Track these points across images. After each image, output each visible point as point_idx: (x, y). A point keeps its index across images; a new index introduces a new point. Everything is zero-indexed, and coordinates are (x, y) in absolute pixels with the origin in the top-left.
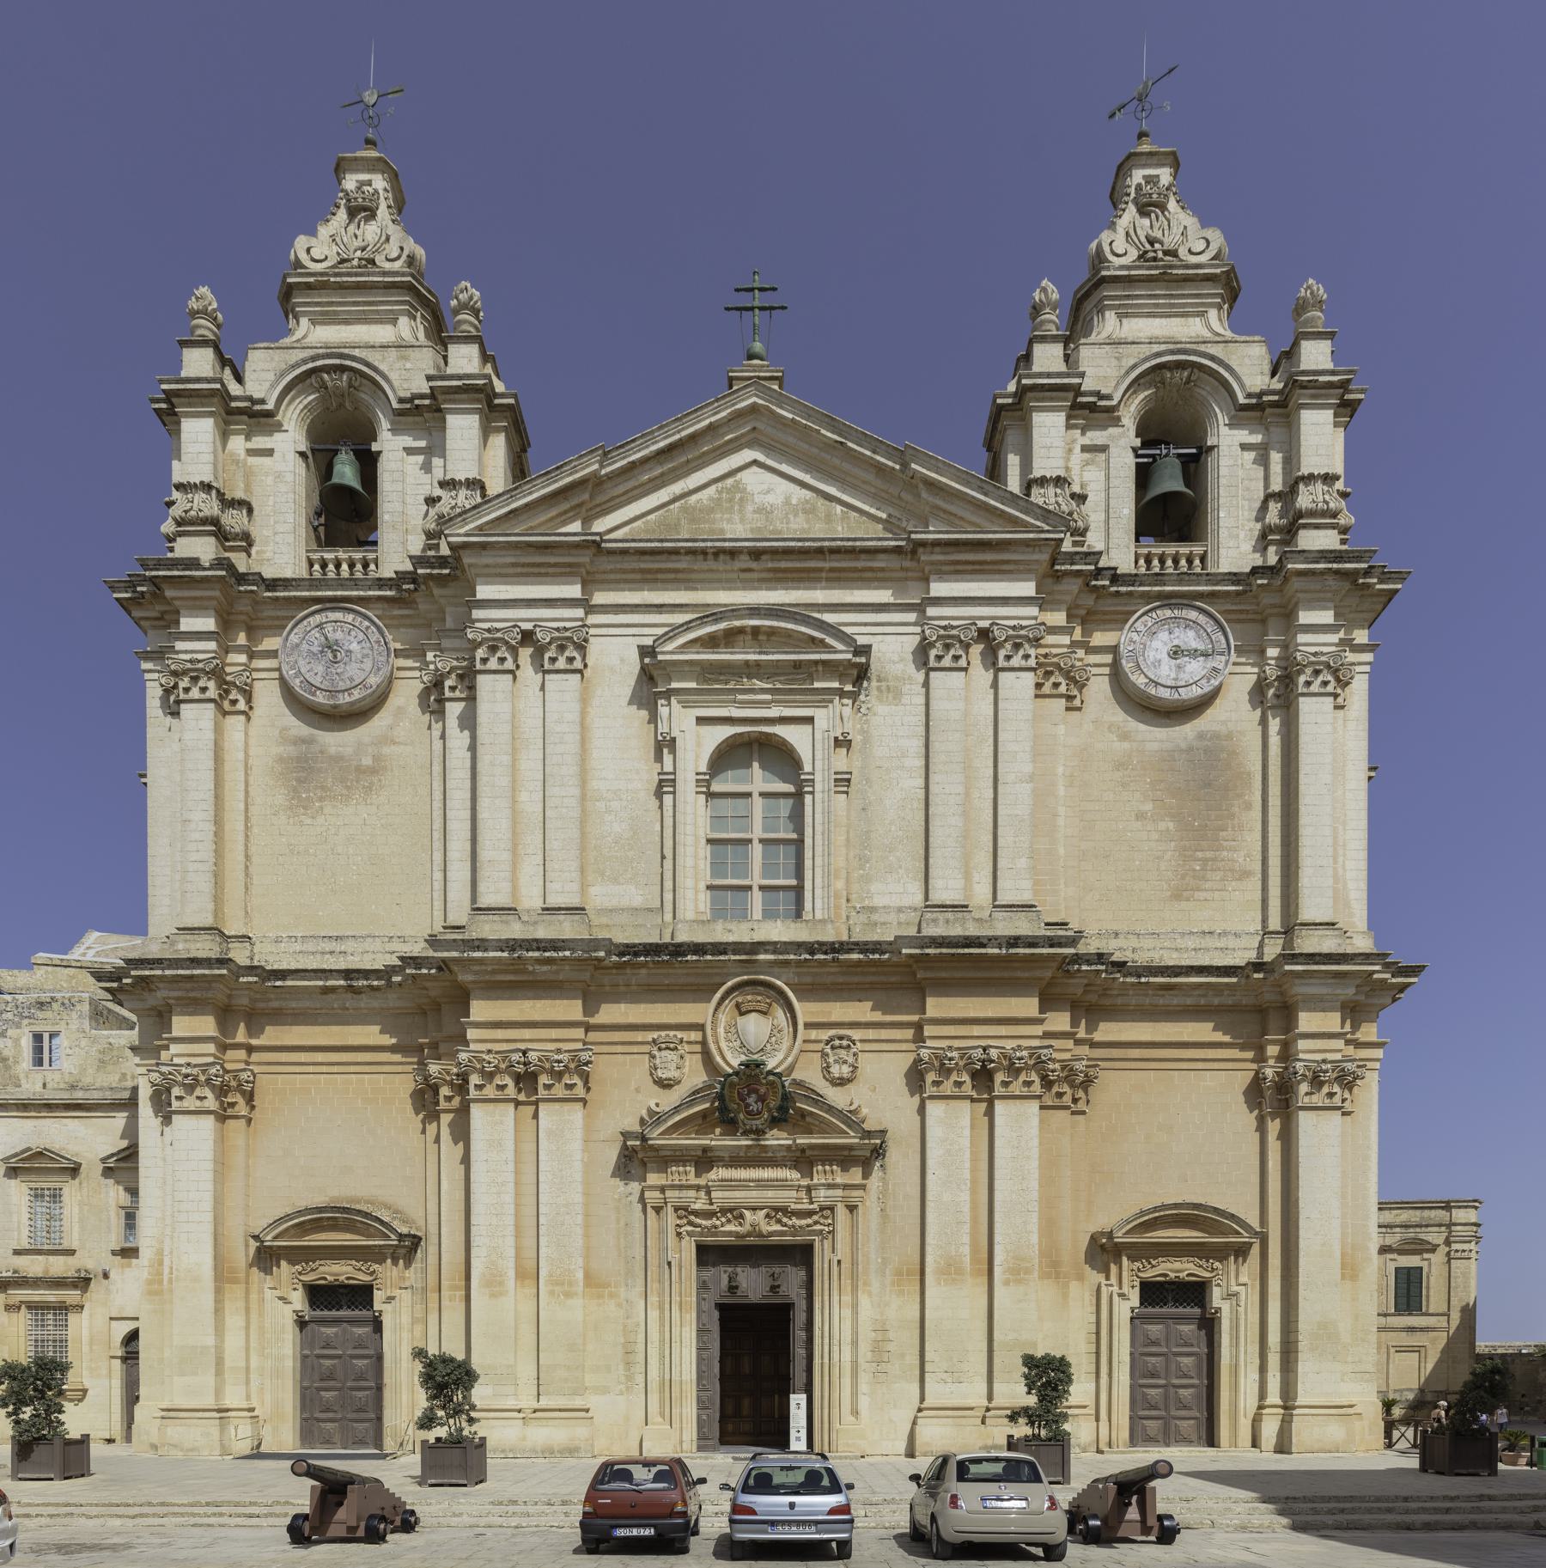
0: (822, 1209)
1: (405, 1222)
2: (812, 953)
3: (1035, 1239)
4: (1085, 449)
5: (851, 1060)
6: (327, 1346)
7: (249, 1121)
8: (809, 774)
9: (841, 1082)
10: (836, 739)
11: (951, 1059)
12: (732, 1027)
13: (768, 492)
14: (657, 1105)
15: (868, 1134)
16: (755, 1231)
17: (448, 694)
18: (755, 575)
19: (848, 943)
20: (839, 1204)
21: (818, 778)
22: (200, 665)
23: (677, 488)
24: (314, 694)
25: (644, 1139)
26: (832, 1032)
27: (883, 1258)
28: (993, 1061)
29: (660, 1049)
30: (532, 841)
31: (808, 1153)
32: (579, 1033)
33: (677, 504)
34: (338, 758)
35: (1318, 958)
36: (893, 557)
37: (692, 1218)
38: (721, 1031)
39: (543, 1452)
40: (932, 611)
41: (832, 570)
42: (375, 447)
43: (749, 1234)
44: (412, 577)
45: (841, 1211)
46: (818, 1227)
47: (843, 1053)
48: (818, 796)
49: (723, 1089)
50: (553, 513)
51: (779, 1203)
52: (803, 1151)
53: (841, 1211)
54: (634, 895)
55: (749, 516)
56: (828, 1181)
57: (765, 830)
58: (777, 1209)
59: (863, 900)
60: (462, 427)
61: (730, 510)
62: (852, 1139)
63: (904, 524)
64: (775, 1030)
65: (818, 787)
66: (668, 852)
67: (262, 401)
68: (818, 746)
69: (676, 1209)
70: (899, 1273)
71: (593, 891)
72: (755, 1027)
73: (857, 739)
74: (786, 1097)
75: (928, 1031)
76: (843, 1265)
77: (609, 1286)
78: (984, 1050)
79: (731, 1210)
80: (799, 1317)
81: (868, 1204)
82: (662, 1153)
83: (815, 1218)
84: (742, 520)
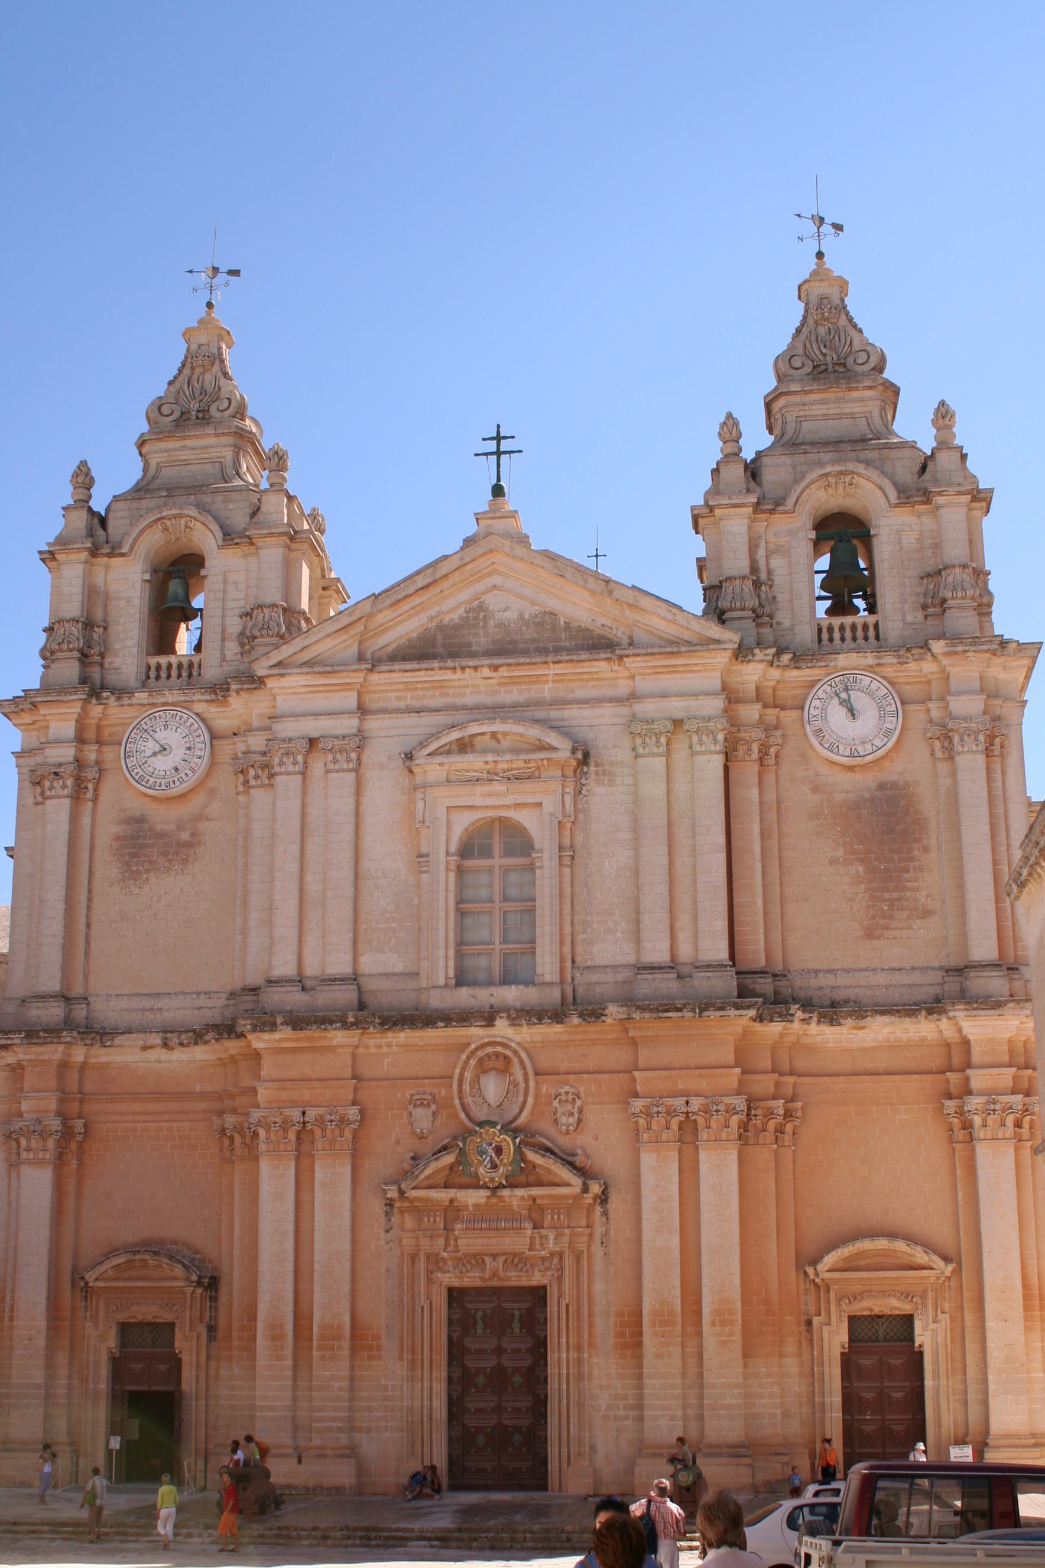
0: (552, 1255)
13: (506, 610)
16: (495, 1274)
18: (495, 681)
21: (546, 855)
29: (415, 1106)
31: (538, 1201)
38: (466, 1087)
40: (638, 708)
43: (490, 1279)
46: (549, 1273)
47: (569, 1107)
54: (395, 962)
58: (515, 1255)
65: (546, 863)
69: (428, 1257)
76: (571, 1309)
79: (474, 1256)
83: (547, 1264)
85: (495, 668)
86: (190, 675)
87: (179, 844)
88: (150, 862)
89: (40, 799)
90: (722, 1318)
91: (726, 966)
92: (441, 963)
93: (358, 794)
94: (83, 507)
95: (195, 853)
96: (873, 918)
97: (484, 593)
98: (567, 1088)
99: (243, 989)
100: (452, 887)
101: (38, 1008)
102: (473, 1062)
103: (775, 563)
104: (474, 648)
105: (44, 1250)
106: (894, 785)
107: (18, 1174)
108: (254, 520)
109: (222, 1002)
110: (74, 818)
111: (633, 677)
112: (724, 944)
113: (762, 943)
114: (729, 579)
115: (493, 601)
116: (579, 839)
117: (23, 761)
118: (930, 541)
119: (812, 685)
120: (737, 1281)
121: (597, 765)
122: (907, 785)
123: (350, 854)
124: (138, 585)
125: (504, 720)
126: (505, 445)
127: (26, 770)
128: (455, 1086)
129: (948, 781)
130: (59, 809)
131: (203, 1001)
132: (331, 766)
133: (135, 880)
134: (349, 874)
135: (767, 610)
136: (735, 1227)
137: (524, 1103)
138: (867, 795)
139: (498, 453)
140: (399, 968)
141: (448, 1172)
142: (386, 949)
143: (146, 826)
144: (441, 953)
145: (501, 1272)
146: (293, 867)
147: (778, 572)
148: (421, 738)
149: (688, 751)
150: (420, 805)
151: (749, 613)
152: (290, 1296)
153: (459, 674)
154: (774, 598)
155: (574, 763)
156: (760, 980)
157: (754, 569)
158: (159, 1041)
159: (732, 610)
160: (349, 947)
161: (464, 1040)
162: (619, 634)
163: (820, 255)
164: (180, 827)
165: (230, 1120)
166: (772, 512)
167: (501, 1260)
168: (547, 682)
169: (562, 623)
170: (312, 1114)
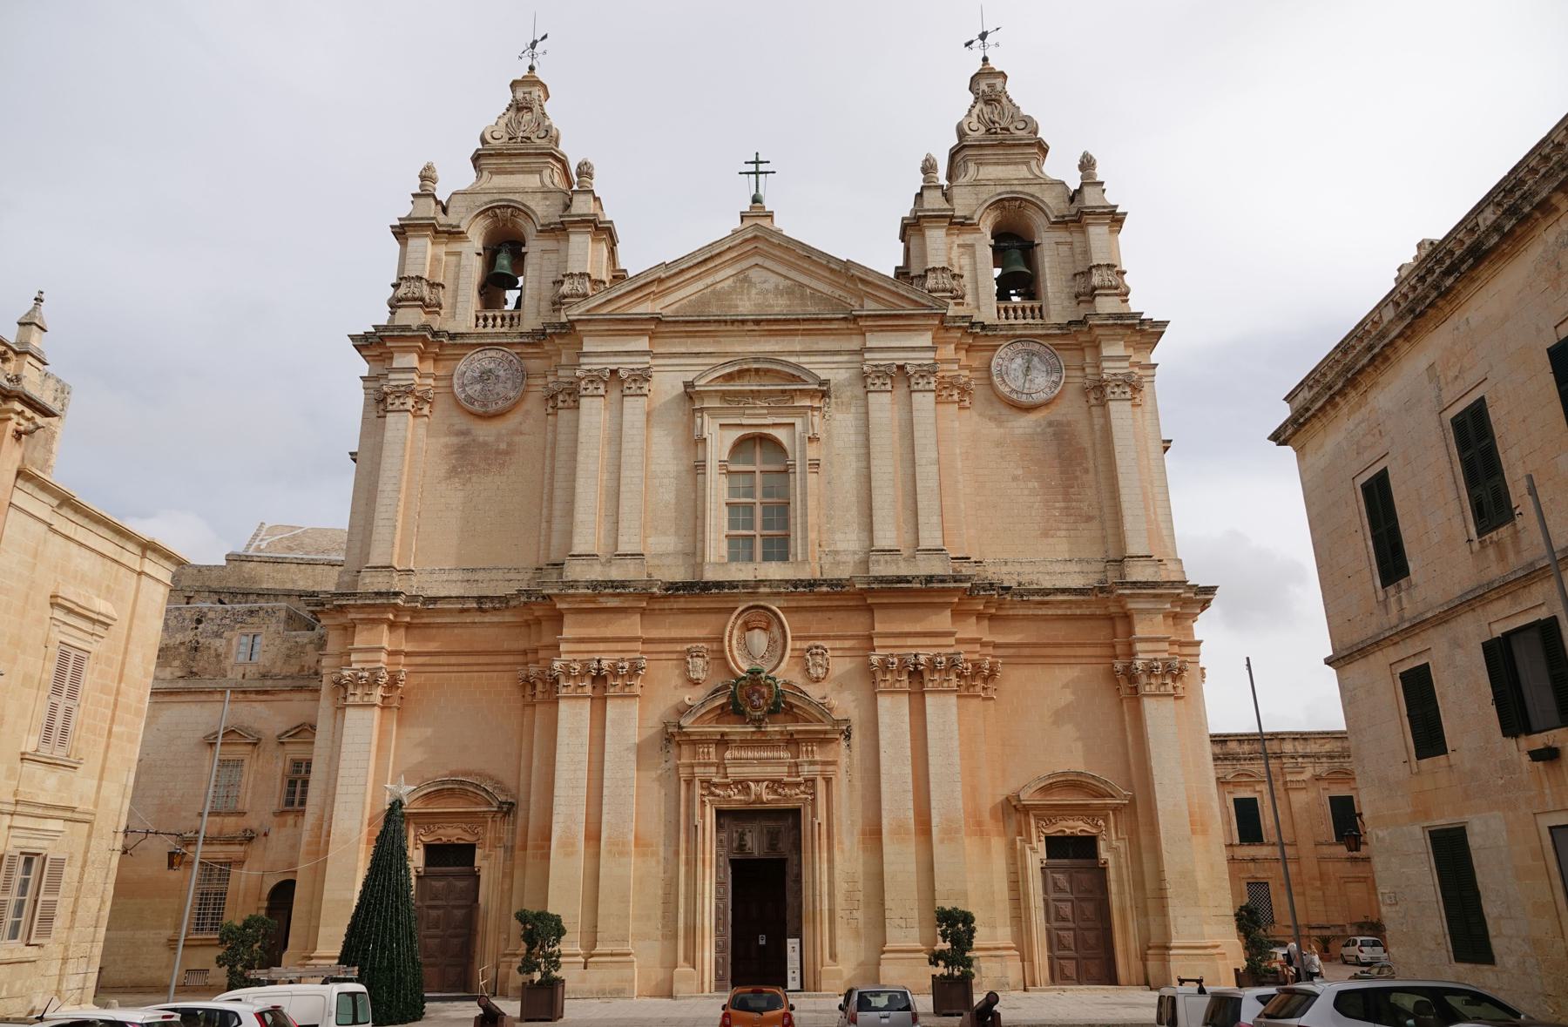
1: (503, 790)
2: (796, 588)
3: (960, 804)
4: (959, 246)
5: (825, 663)
6: (435, 898)
9: (817, 680)
10: (809, 438)
12: (742, 638)
16: (759, 800)
17: (560, 404)
18: (757, 333)
20: (818, 777)
21: (798, 463)
23: (709, 281)
24: (473, 404)
25: (680, 727)
26: (811, 643)
27: (852, 821)
32: (639, 646)
34: (485, 444)
36: (842, 322)
37: (713, 789)
38: (734, 642)
39: (597, 993)
40: (867, 356)
41: (804, 330)
42: (524, 250)
43: (754, 802)
45: (821, 785)
47: (819, 659)
48: (798, 475)
50: (634, 298)
52: (792, 735)
55: (753, 296)
56: (811, 762)
57: (765, 527)
58: (774, 781)
61: (742, 293)
63: (849, 301)
64: (772, 642)
65: (798, 470)
66: (699, 514)
72: (759, 640)
73: (822, 436)
74: (780, 694)
75: (876, 642)
77: (652, 846)
79: (741, 782)
80: (791, 870)
81: (839, 776)
82: (692, 738)
84: (749, 299)
96: (1048, 522)
97: (747, 269)
98: (818, 643)
101: (371, 576)
104: (740, 309)
109: (530, 575)
111: (864, 335)
112: (939, 534)
121: (836, 398)
122: (1069, 424)
129: (1102, 421)
132: (628, 392)
136: (957, 760)
141: (719, 711)
149: (907, 389)
153: (729, 327)
158: (475, 605)
161: (731, 605)
162: (852, 303)
163: (985, 59)
165: (533, 670)
167: (766, 783)
168: (797, 335)
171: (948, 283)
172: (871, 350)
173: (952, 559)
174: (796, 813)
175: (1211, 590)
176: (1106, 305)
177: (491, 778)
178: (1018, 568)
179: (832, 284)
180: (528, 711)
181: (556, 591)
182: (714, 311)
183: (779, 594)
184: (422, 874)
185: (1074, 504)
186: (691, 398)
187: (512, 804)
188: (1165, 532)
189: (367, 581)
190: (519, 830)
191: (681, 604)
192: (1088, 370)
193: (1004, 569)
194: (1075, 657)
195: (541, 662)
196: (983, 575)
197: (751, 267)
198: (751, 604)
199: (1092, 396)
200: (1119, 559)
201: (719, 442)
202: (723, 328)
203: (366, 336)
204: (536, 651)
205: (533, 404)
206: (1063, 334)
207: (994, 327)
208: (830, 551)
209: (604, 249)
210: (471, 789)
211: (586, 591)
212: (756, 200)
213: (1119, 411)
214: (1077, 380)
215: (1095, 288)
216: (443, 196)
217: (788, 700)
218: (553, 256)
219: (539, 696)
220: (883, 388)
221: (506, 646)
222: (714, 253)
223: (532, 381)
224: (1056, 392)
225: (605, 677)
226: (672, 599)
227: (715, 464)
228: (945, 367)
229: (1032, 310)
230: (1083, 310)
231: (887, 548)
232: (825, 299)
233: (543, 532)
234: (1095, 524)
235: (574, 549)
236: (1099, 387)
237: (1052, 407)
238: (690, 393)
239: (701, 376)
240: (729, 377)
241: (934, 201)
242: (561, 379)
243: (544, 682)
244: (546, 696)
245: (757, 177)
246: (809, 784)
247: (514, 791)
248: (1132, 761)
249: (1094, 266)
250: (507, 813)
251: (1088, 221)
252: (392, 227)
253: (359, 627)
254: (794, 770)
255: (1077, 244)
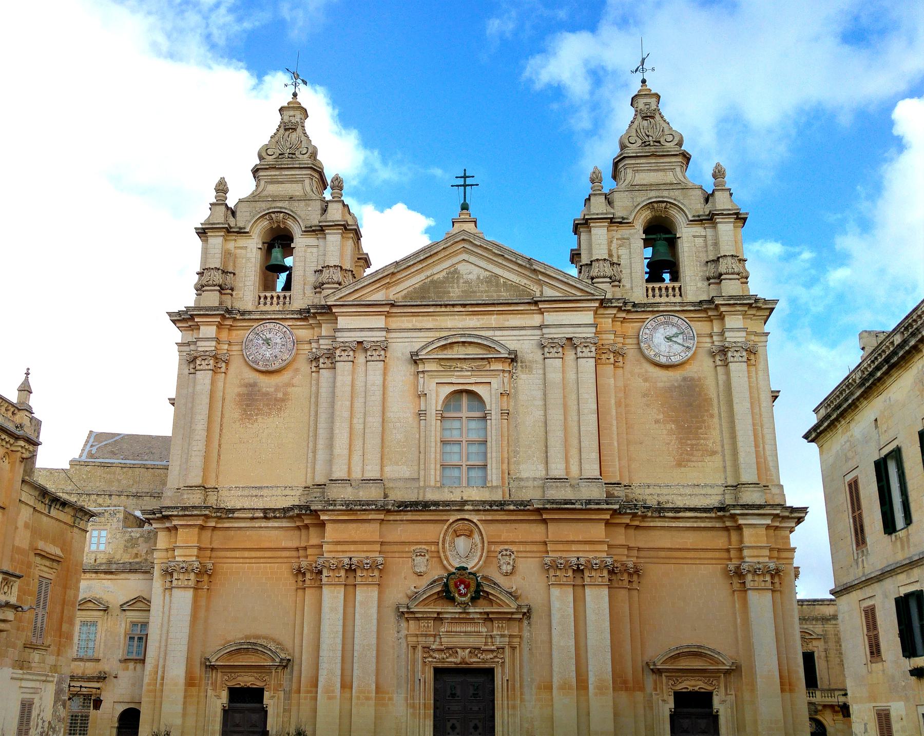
7: (208, 589)
8: (489, 410)
9: (506, 574)
10: (501, 393)
11: (561, 564)
14: (415, 587)
15: (519, 607)
17: (321, 366)
19: (508, 501)
20: (507, 647)
21: (493, 413)
22: (207, 353)
23: (429, 273)
25: (408, 608)
27: (531, 679)
28: (582, 565)
29: (417, 556)
30: (358, 444)
33: (429, 280)
35: (747, 507)
37: (431, 653)
38: (447, 545)
40: (545, 331)
43: (460, 663)
44: (308, 311)
45: (507, 650)
48: (493, 421)
49: (447, 581)
51: (476, 645)
52: (487, 613)
53: (507, 650)
55: (461, 285)
58: (475, 649)
59: (516, 473)
60: (334, 238)
62: (513, 607)
65: (494, 417)
67: (244, 228)
68: (493, 397)
69: (424, 648)
70: (539, 688)
71: (387, 469)
72: (462, 543)
74: (479, 585)
76: (510, 683)
78: (578, 559)
82: (417, 615)
83: (495, 654)
84: (458, 287)
85: (464, 305)
86: (284, 303)
87: (276, 399)
88: (258, 409)
89: (192, 371)
90: (601, 689)
91: (599, 479)
92: (433, 472)
93: (385, 375)
94: (222, 204)
95: (286, 405)
98: (506, 547)
99: (313, 485)
100: (439, 428)
102: (451, 530)
103: (620, 252)
105: (185, 641)
106: (692, 379)
107: (171, 595)
108: (324, 217)
110: (213, 383)
111: (542, 313)
112: (597, 466)
113: (617, 466)
114: (597, 260)
115: (463, 268)
116: (512, 403)
117: (187, 349)
118: (711, 242)
119: (643, 320)
120: (610, 669)
122: (699, 379)
123: (380, 408)
124: (255, 250)
125: (470, 336)
126: (469, 181)
127: (185, 354)
128: (440, 544)
130: (204, 378)
131: (288, 492)
133: (249, 419)
134: (381, 420)
135: (618, 278)
136: (608, 636)
137: (481, 556)
138: (676, 384)
139: (465, 186)
140: (407, 475)
142: (400, 463)
143: (257, 389)
144: (433, 466)
145: (467, 660)
146: (346, 414)
147: (623, 257)
148: (423, 344)
149: (574, 356)
150: (421, 381)
151: (608, 280)
152: (339, 672)
153: (443, 309)
154: (621, 271)
155: (510, 360)
156: (618, 489)
157: (611, 255)
158: (262, 515)
159: (596, 278)
160: (379, 461)
161: (445, 518)
164: (277, 390)
165: (304, 564)
166: (620, 223)
168: (493, 314)
169: (502, 282)
170: (354, 561)
171: (608, 271)
172: (547, 326)
173: (605, 484)
174: (490, 672)
175: (804, 510)
176: (731, 288)
177: (274, 641)
178: (658, 491)
179: (519, 274)
180: (300, 592)
181: (320, 507)
182: (433, 298)
183: (479, 510)
184: (227, 708)
185: (702, 441)
186: (415, 362)
187: (289, 660)
188: (771, 464)
189: (185, 496)
190: (295, 680)
191: (409, 517)
192: (715, 338)
193: (648, 491)
194: (700, 559)
195: (309, 557)
196: (631, 496)
197: (460, 262)
198: (459, 518)
199: (718, 358)
200: (735, 484)
201: (438, 394)
202: (438, 309)
203: (179, 313)
204: (305, 548)
205: (304, 367)
206: (695, 310)
207: (645, 305)
208: (516, 478)
209: (350, 244)
210: (260, 649)
211: (341, 507)
212: (465, 207)
213: (738, 369)
214: (706, 345)
215: (721, 275)
216: (231, 203)
217: (485, 589)
218: (315, 250)
219: (308, 582)
220: (556, 355)
221: (284, 545)
222: (432, 253)
223: (300, 347)
224: (689, 355)
225: (355, 570)
226: (402, 513)
227: (434, 412)
228: (604, 336)
229: (674, 288)
230: (713, 291)
231: (557, 477)
232: (514, 286)
233: (310, 460)
234: (718, 458)
235: (333, 475)
236: (724, 351)
237: (687, 366)
238: (415, 359)
239: (423, 348)
240: (444, 347)
241: (599, 207)
242: (321, 347)
243: (312, 572)
244: (313, 582)
245: (465, 189)
246: (501, 651)
247: (291, 651)
248: (740, 637)
249: (721, 257)
250: (285, 667)
251: (717, 220)
252: (196, 229)
253: (180, 531)
254: (489, 640)
255: (709, 238)
